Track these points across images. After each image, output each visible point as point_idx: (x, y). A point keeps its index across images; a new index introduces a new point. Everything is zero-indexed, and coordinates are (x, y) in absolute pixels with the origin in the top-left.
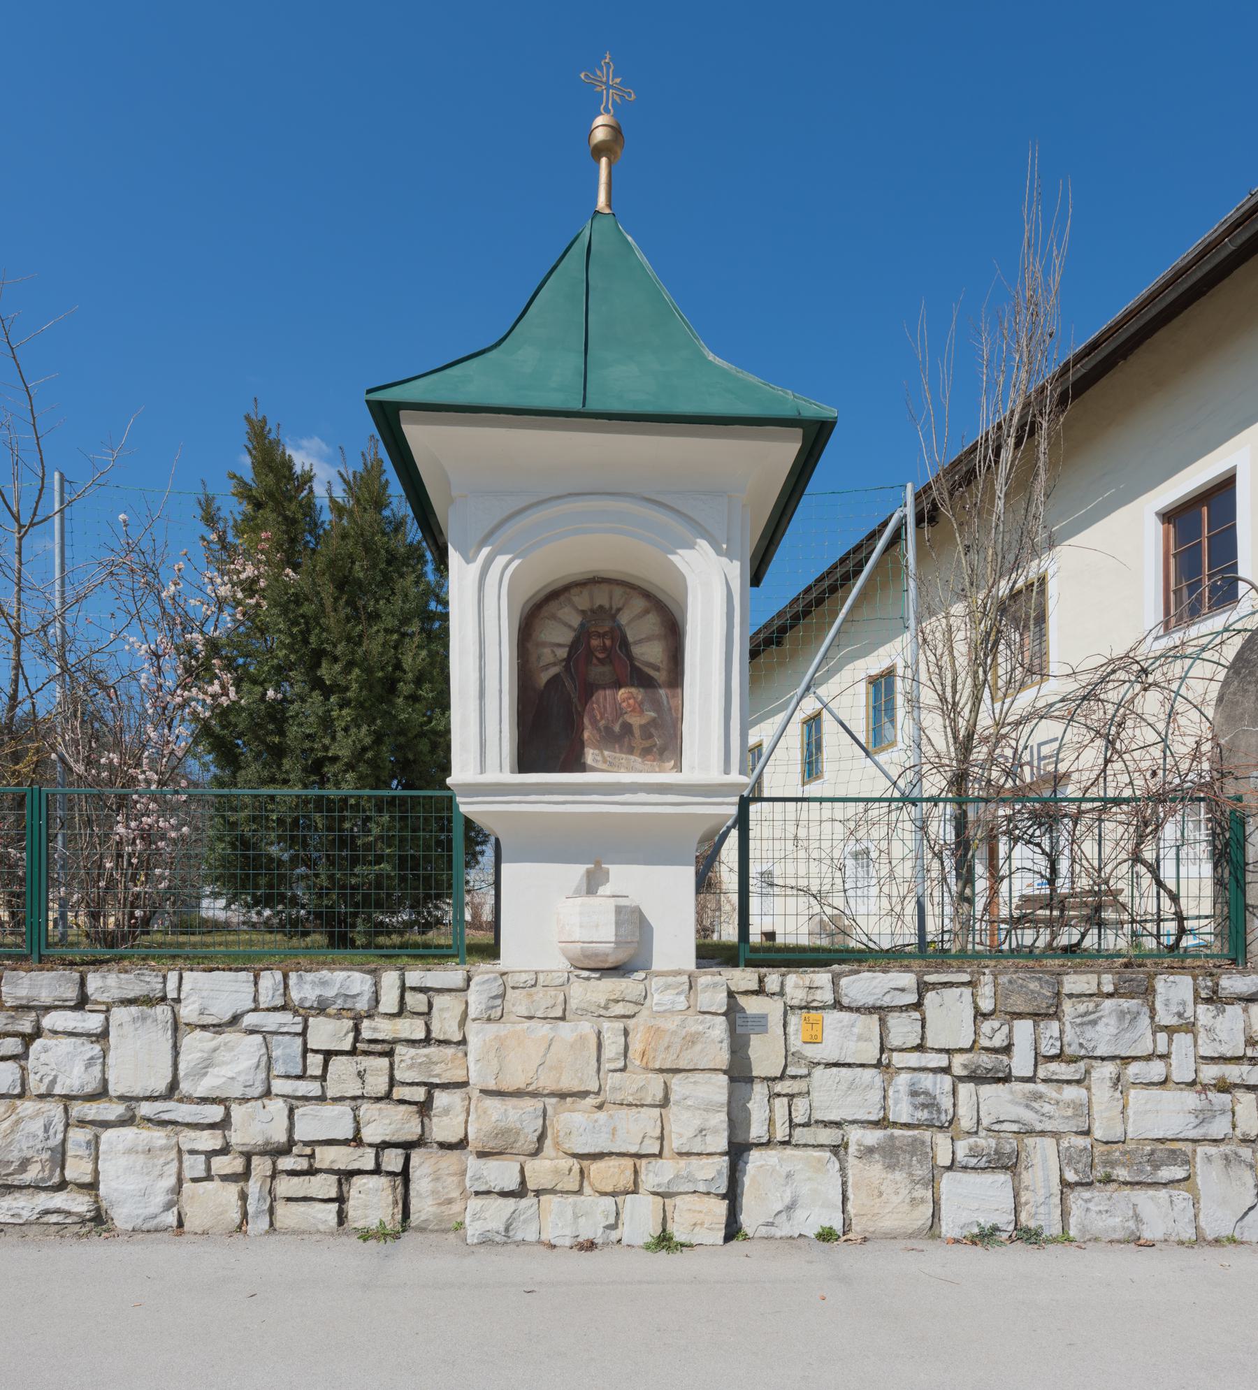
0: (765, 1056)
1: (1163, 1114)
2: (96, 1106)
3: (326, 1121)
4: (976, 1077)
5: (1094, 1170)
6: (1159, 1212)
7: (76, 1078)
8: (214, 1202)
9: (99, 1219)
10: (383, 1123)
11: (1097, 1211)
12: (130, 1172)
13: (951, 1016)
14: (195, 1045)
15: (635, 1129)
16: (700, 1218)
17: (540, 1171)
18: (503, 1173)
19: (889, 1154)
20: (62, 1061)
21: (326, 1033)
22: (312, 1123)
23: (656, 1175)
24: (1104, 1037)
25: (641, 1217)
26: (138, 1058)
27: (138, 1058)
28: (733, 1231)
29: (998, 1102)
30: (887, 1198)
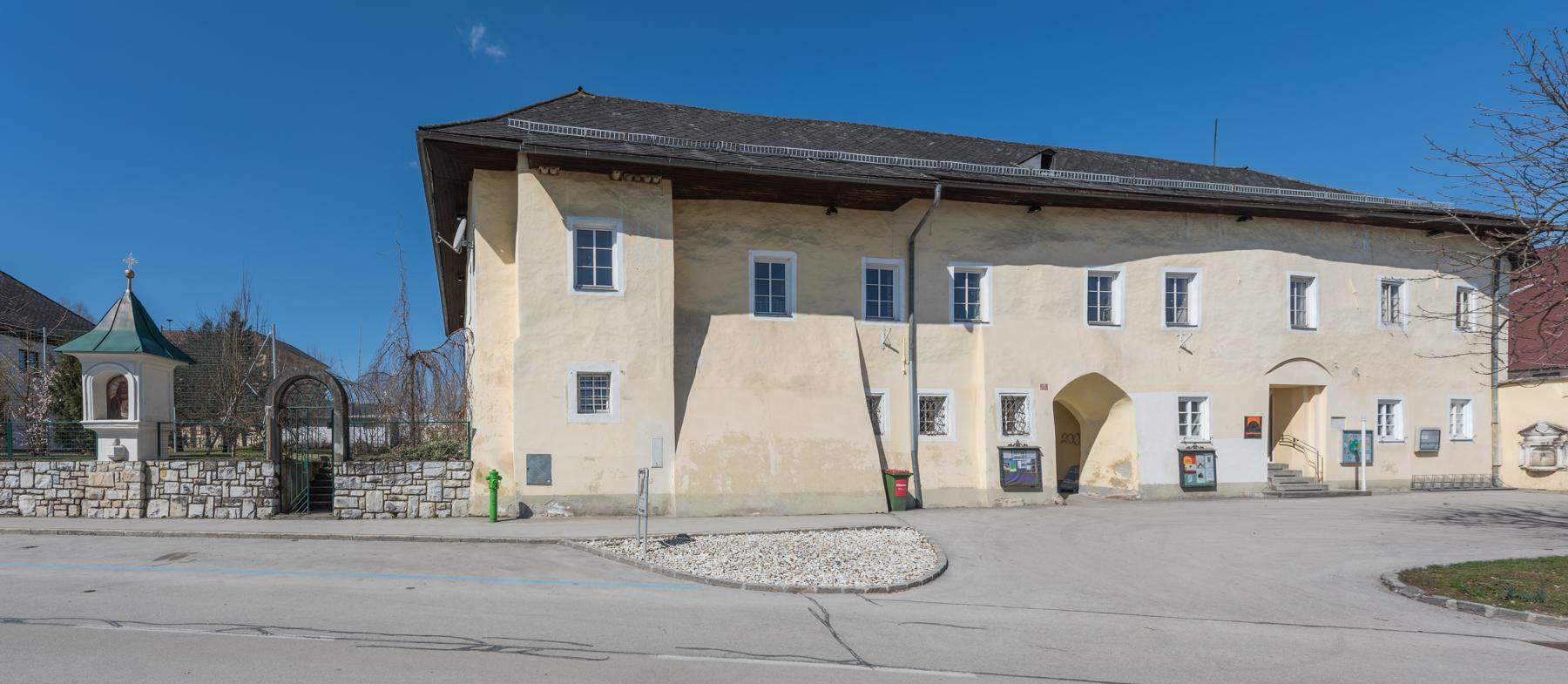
0: (155, 480)
1: (237, 492)
2: (18, 490)
3: (65, 493)
4: (200, 484)
5: (221, 503)
6: (232, 511)
7: (13, 484)
8: (42, 510)
9: (20, 514)
10: (75, 494)
11: (220, 512)
12: (24, 504)
13: (193, 471)
14: (38, 477)
15: (121, 494)
16: (135, 513)
17: (103, 503)
18: (95, 503)
19: (179, 500)
20: (11, 481)
21: (64, 475)
22: (62, 494)
23: (127, 503)
24: (224, 475)
25: (123, 512)
26: (26, 480)
27: (26, 480)
28: (144, 515)
29: (203, 489)
30: (178, 509)
